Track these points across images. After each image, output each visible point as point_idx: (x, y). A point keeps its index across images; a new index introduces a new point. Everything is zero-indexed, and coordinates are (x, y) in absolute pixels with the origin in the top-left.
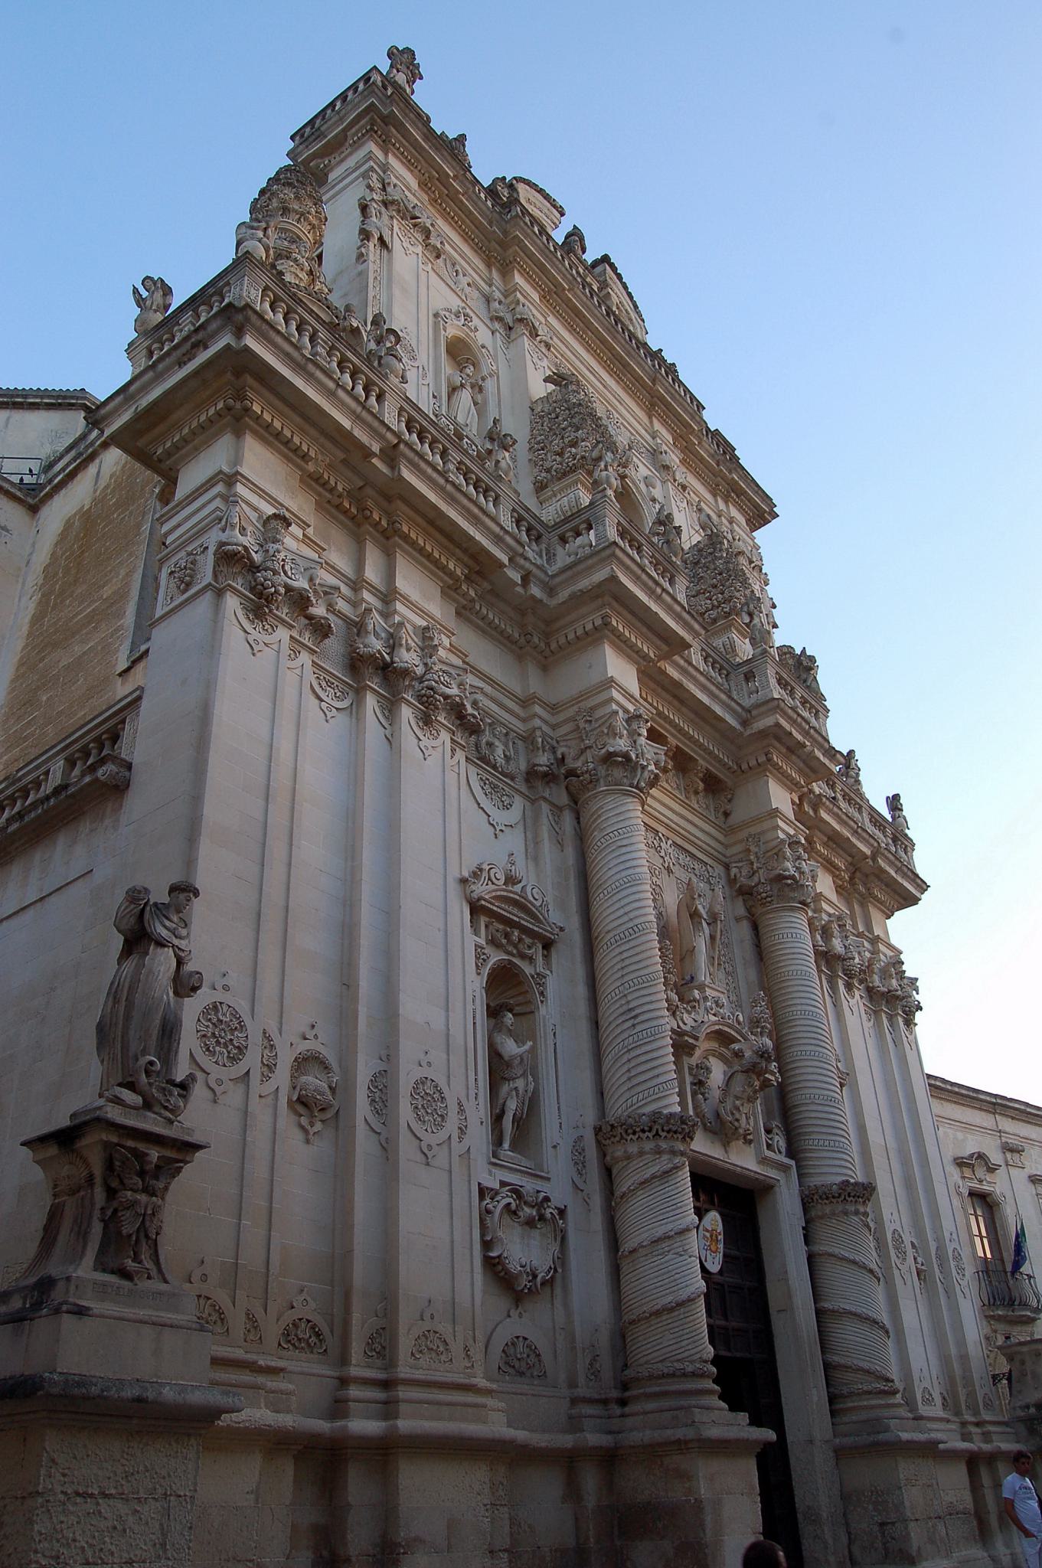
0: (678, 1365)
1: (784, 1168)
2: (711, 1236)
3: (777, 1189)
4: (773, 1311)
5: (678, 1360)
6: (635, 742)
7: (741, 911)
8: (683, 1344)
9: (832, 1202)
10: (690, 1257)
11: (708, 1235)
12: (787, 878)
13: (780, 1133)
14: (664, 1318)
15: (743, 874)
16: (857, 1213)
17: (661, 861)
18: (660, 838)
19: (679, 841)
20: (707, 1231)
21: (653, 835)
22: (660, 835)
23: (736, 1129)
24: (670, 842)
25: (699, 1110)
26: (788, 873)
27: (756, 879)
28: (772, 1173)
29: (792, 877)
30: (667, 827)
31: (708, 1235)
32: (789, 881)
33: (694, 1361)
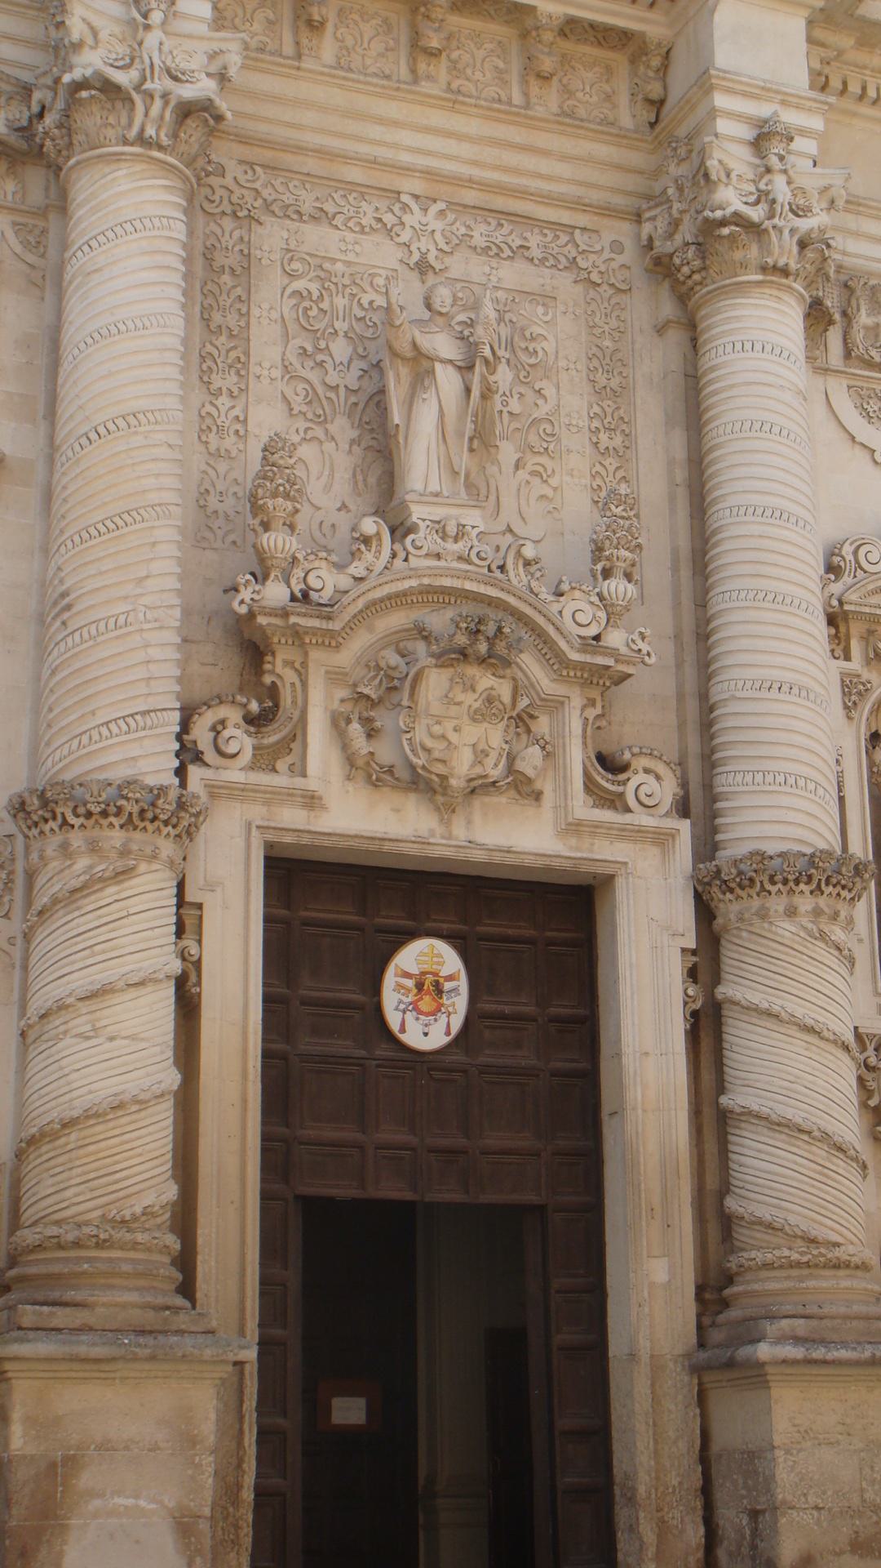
0: (54, 1231)
1: (662, 840)
2: (420, 986)
3: (620, 883)
4: (606, 1109)
5: (58, 1223)
6: (140, 44)
7: (668, 308)
8: (68, 1193)
9: (738, 897)
10: (111, 1039)
11: (410, 983)
12: (723, 223)
13: (661, 768)
14: (44, 1149)
15: (660, 231)
16: (791, 912)
17: (400, 253)
18: (405, 207)
19: (470, 197)
20: (407, 975)
21: (383, 204)
22: (405, 198)
23: (443, 778)
24: (435, 208)
25: (349, 752)
26: (718, 214)
27: (678, 239)
28: (604, 852)
29: (738, 219)
30: (429, 174)
31: (410, 983)
32: (725, 231)
33: (87, 1223)
